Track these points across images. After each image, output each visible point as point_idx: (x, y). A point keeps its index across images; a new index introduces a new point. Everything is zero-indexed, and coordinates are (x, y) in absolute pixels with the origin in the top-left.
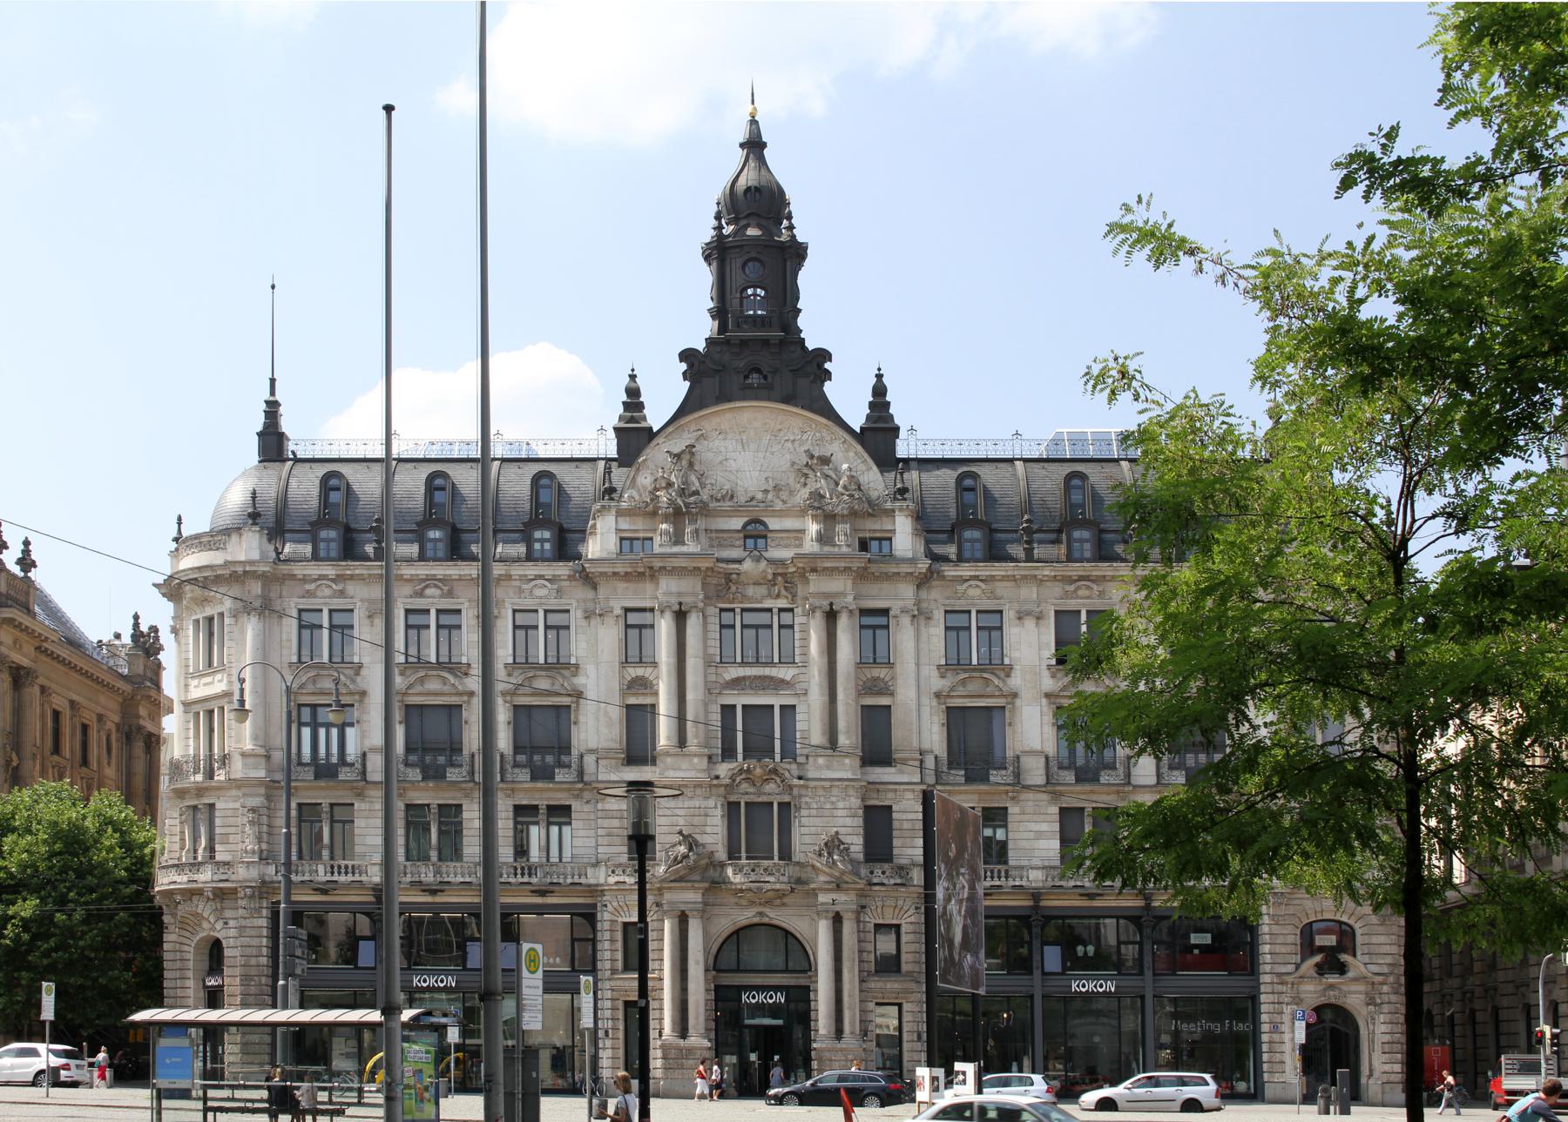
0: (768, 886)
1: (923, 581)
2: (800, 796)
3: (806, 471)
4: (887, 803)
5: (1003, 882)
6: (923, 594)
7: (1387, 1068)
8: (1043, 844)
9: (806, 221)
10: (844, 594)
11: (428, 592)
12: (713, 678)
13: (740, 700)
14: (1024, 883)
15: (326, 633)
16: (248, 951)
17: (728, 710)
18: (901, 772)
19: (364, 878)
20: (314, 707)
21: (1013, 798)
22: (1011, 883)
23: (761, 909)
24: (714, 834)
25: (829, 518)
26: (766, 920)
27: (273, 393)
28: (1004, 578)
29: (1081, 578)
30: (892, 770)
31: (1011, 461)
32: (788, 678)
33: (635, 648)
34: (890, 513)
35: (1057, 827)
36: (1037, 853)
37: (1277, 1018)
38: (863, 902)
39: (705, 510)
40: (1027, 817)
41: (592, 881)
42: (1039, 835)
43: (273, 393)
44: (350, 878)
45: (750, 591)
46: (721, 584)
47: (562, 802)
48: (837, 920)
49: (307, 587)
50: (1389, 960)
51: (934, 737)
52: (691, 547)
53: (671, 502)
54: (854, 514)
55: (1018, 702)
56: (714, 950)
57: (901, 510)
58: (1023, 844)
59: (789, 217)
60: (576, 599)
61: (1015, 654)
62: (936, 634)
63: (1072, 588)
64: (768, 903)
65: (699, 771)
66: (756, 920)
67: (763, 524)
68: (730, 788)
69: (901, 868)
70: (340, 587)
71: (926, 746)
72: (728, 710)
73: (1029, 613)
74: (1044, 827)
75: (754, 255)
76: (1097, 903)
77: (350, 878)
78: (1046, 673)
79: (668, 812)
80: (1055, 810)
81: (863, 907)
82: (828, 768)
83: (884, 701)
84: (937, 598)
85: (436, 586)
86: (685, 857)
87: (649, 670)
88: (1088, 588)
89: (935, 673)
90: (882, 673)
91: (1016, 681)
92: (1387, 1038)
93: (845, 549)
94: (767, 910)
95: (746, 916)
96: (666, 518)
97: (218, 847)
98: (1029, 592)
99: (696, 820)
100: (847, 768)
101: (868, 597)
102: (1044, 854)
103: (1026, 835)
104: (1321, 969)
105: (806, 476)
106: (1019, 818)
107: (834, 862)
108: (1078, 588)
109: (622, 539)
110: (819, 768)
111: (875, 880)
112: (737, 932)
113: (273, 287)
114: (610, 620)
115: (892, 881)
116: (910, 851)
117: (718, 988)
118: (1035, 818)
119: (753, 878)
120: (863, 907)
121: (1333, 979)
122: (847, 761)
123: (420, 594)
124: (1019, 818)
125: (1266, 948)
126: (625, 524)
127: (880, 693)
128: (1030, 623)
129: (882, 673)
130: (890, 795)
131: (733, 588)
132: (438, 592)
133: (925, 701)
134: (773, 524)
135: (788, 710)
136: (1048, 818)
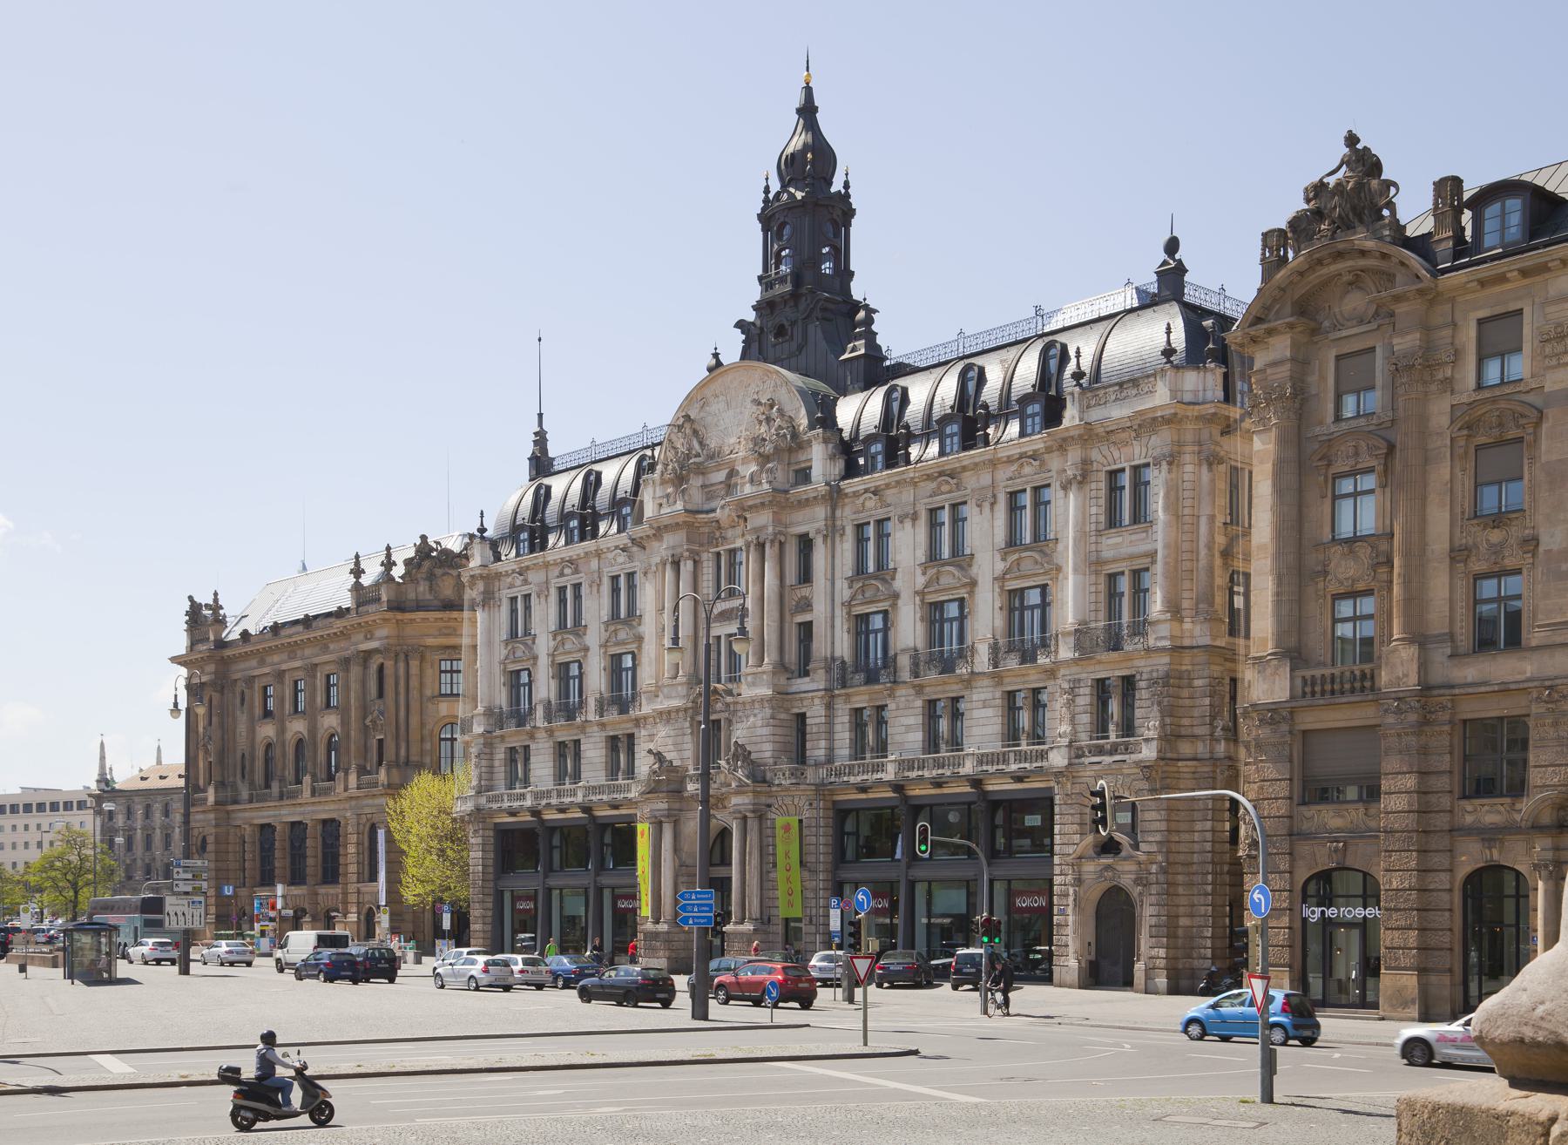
2: (735, 711)
7: (1154, 952)
9: (857, 171)
10: (765, 527)
18: (813, 681)
27: (540, 424)
30: (807, 679)
35: (920, 719)
36: (907, 746)
39: (701, 470)
42: (909, 729)
43: (540, 424)
50: (1158, 837)
51: (843, 647)
55: (900, 603)
58: (898, 738)
61: (898, 558)
62: (847, 547)
71: (838, 654)
73: (906, 516)
76: (946, 791)
78: (919, 571)
80: (919, 703)
89: (846, 585)
91: (898, 584)
92: (1154, 921)
98: (908, 495)
101: (799, 524)
121: (1106, 860)
123: (562, 574)
128: (908, 524)
133: (838, 612)
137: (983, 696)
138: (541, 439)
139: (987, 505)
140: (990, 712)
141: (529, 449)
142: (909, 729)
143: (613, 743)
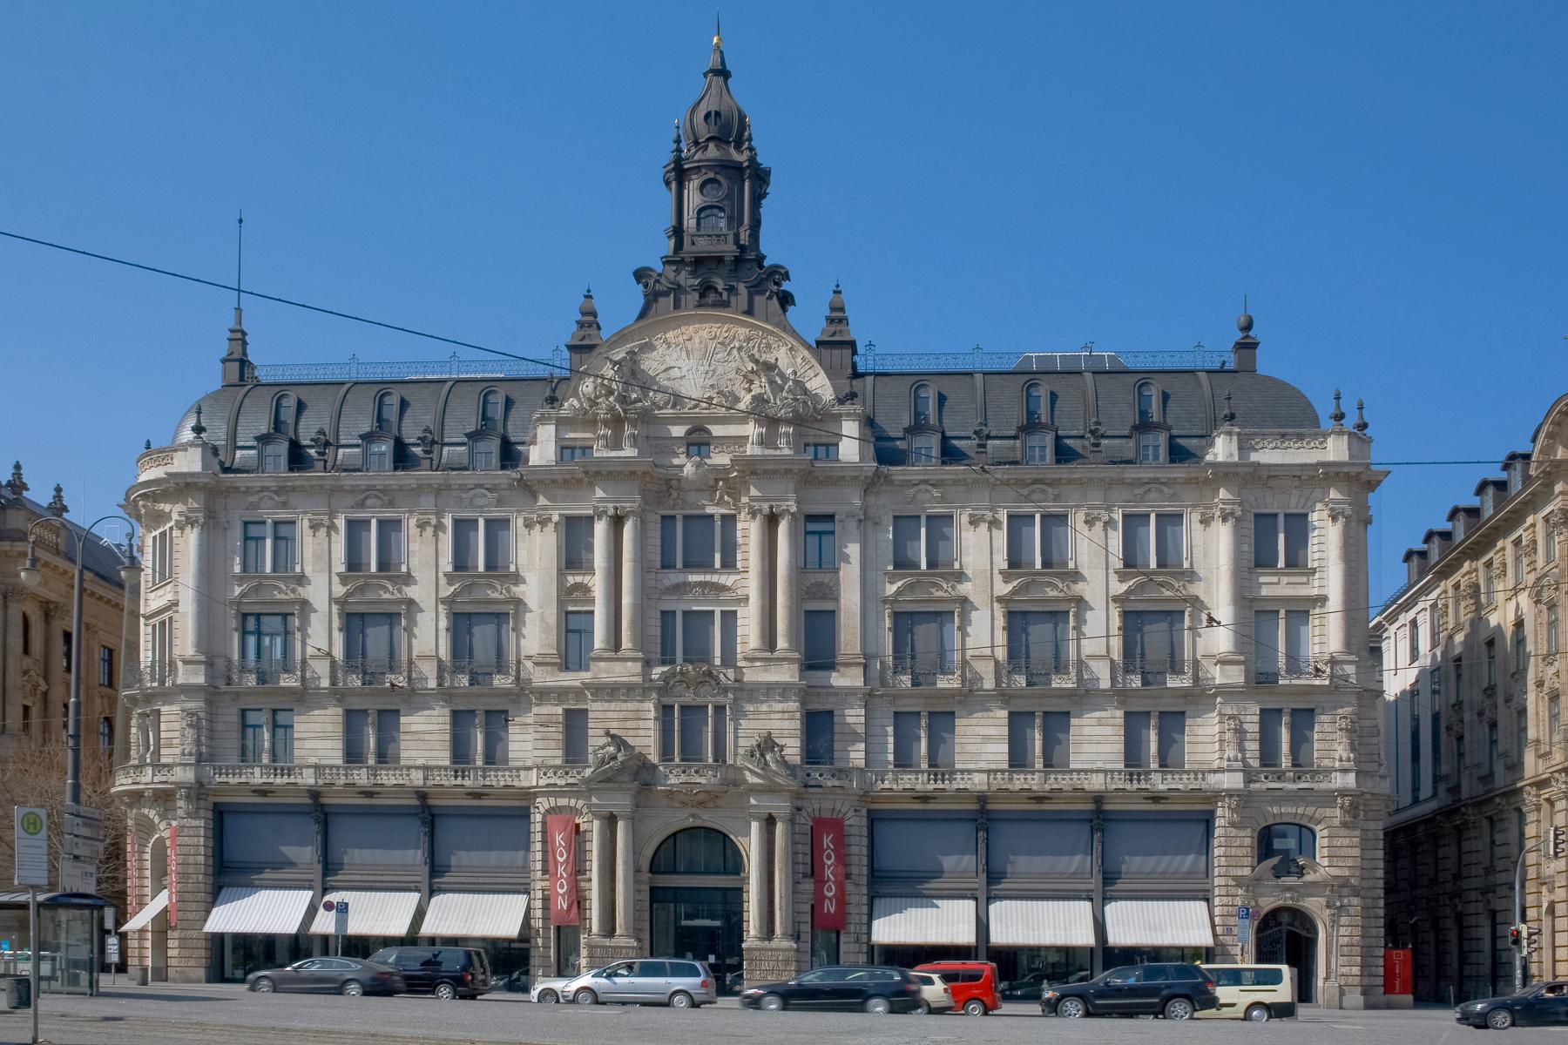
1: (871, 485)
3: (751, 376)
4: (828, 707)
5: (947, 785)
6: (871, 499)
8: (991, 748)
11: (369, 502)
12: (652, 583)
15: (269, 542)
16: (185, 850)
17: (667, 616)
18: (844, 675)
19: (299, 781)
20: (258, 616)
21: (960, 703)
22: (955, 786)
23: (694, 811)
24: (646, 739)
25: (772, 422)
26: (699, 823)
28: (955, 482)
29: (1035, 481)
31: (970, 374)
32: (729, 584)
33: (573, 557)
34: (838, 418)
35: (1005, 731)
38: (799, 804)
41: (525, 784)
42: (987, 739)
44: (285, 780)
45: (692, 497)
46: (659, 489)
47: (499, 708)
48: (770, 822)
49: (251, 499)
52: (629, 452)
53: (611, 409)
54: (798, 421)
56: (649, 852)
57: (848, 415)
58: (971, 748)
59: (750, 139)
63: (1025, 491)
64: (701, 804)
66: (691, 822)
67: (708, 432)
68: (665, 688)
70: (282, 499)
72: (667, 616)
74: (992, 731)
75: (711, 175)
77: (285, 780)
79: (600, 715)
80: (1004, 713)
81: (799, 809)
83: (828, 606)
84: (886, 505)
85: (377, 497)
86: (614, 758)
88: (1043, 491)
90: (826, 578)
93: (787, 452)
94: (700, 812)
95: (681, 819)
96: (606, 423)
97: (163, 751)
99: (629, 724)
100: (786, 674)
104: (1278, 872)
105: (751, 382)
107: (766, 763)
108: (1033, 492)
109: (563, 448)
112: (674, 835)
113: (241, 221)
114: (551, 527)
117: (654, 891)
118: (983, 721)
119: (683, 778)
120: (799, 809)
127: (824, 597)
129: (826, 578)
130: (832, 699)
131: (675, 494)
132: (379, 502)
134: (717, 430)
135: (730, 618)
140: (1108, 730)
142: (987, 739)
143: (460, 719)
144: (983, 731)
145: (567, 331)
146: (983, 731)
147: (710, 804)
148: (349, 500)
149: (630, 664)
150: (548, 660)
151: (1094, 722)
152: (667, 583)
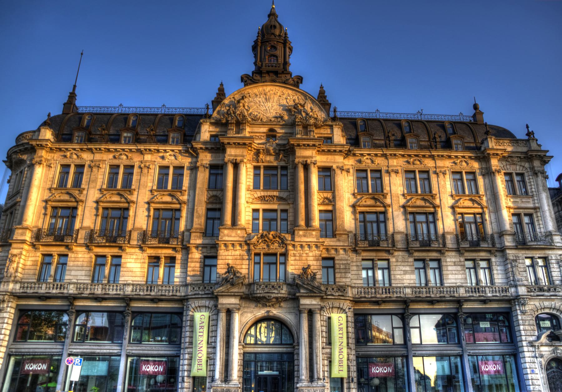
0: (273, 295)
4: (333, 256)
8: (407, 276)
10: (312, 157)
13: (260, 206)
14: (402, 295)
18: (339, 240)
23: (268, 309)
30: (335, 239)
37: (533, 365)
40: (399, 264)
42: (405, 272)
58: (398, 277)
60: (186, 161)
65: (241, 237)
69: (341, 287)
79: (223, 258)
82: (305, 236)
87: (219, 192)
102: (408, 282)
103: (399, 272)
106: (395, 264)
110: (300, 236)
111: (329, 293)
113: (82, 54)
115: (337, 294)
116: (344, 280)
118: (403, 264)
119: (266, 290)
122: (314, 233)
124: (395, 264)
125: (522, 327)
126: (212, 129)
128: (393, 175)
136: (409, 264)
137: (453, 260)
138: (72, 96)
139: (441, 176)
141: (66, 100)
144: (404, 269)
145: (213, 96)
146: (404, 269)
147: (278, 305)
148: (111, 156)
149: (239, 232)
150: (198, 231)
151: (453, 264)
152: (256, 196)
